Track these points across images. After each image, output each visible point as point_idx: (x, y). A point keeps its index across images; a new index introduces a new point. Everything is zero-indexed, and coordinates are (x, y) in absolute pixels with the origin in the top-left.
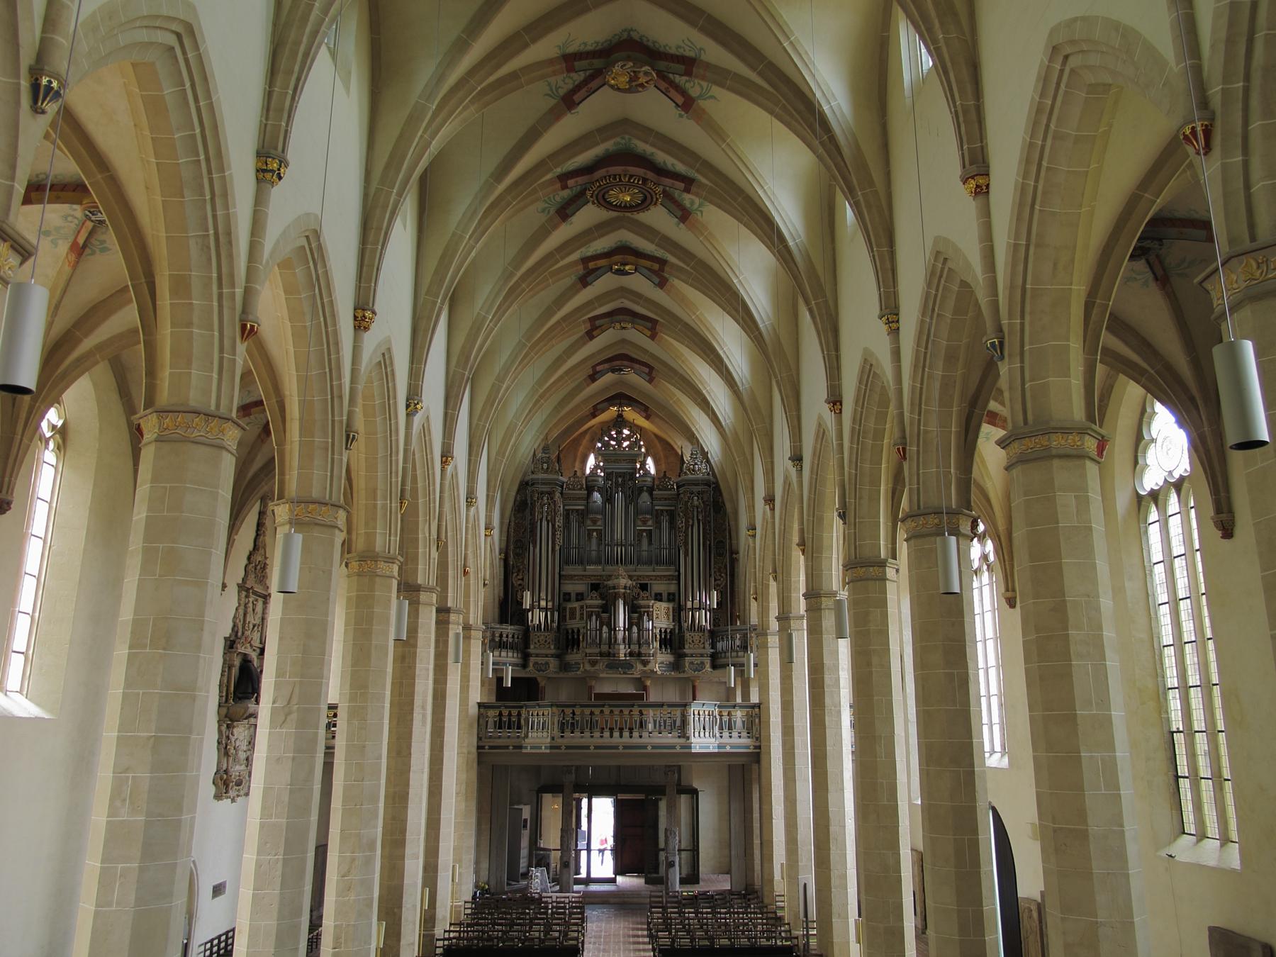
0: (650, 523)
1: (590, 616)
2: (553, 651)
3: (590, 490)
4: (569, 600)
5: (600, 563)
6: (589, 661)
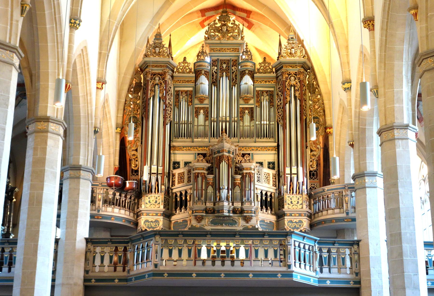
0: (252, 102)
3: (198, 73)
6: (196, 217)
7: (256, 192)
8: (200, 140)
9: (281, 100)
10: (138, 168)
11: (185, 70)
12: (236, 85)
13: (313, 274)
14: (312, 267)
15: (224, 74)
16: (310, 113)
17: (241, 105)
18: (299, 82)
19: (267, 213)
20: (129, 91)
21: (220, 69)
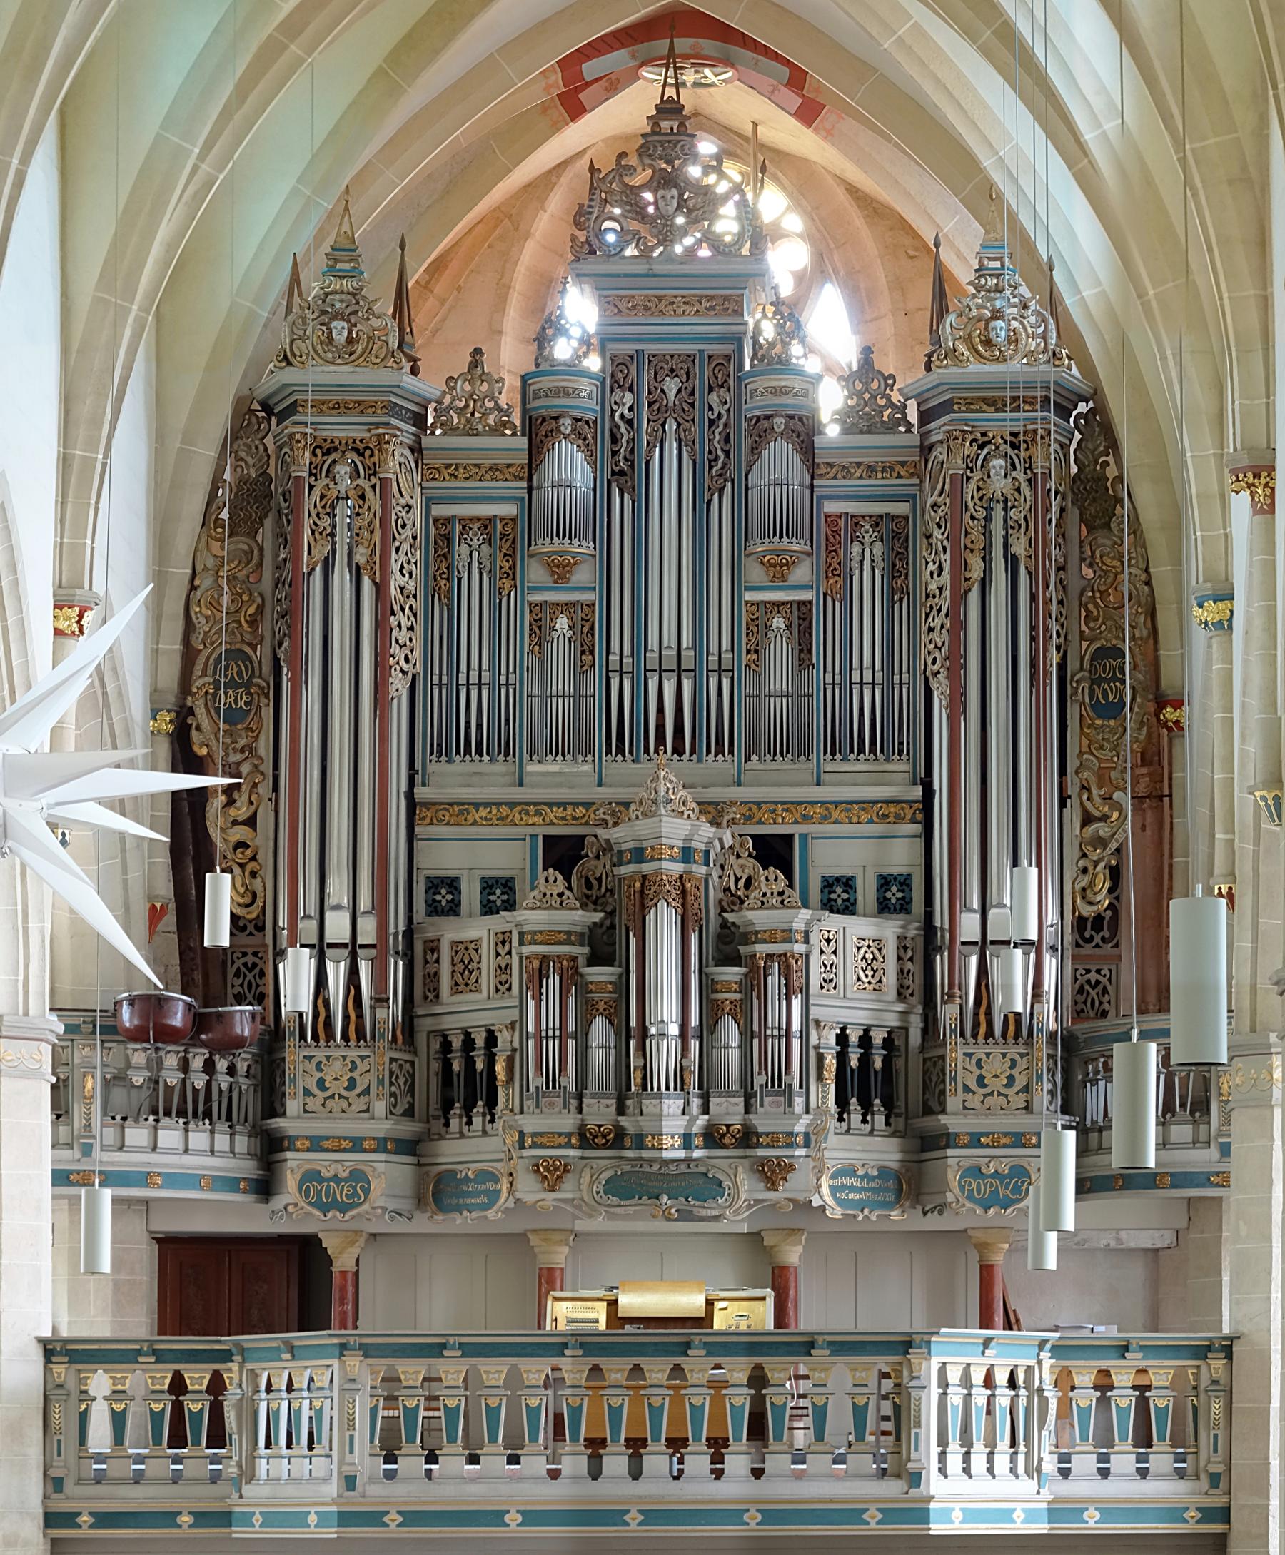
0: (801, 573)
1: (537, 974)
2: (381, 1124)
4: (454, 909)
5: (586, 749)
7: (814, 1040)
8: (554, 768)
9: (941, 568)
10: (264, 908)
11: (477, 415)
12: (729, 484)
13: (1027, 1486)
14: (1021, 1459)
15: (671, 426)
16: (1084, 628)
17: (747, 589)
18: (1029, 481)
19: (868, 1127)
20: (208, 519)
21: (650, 404)
